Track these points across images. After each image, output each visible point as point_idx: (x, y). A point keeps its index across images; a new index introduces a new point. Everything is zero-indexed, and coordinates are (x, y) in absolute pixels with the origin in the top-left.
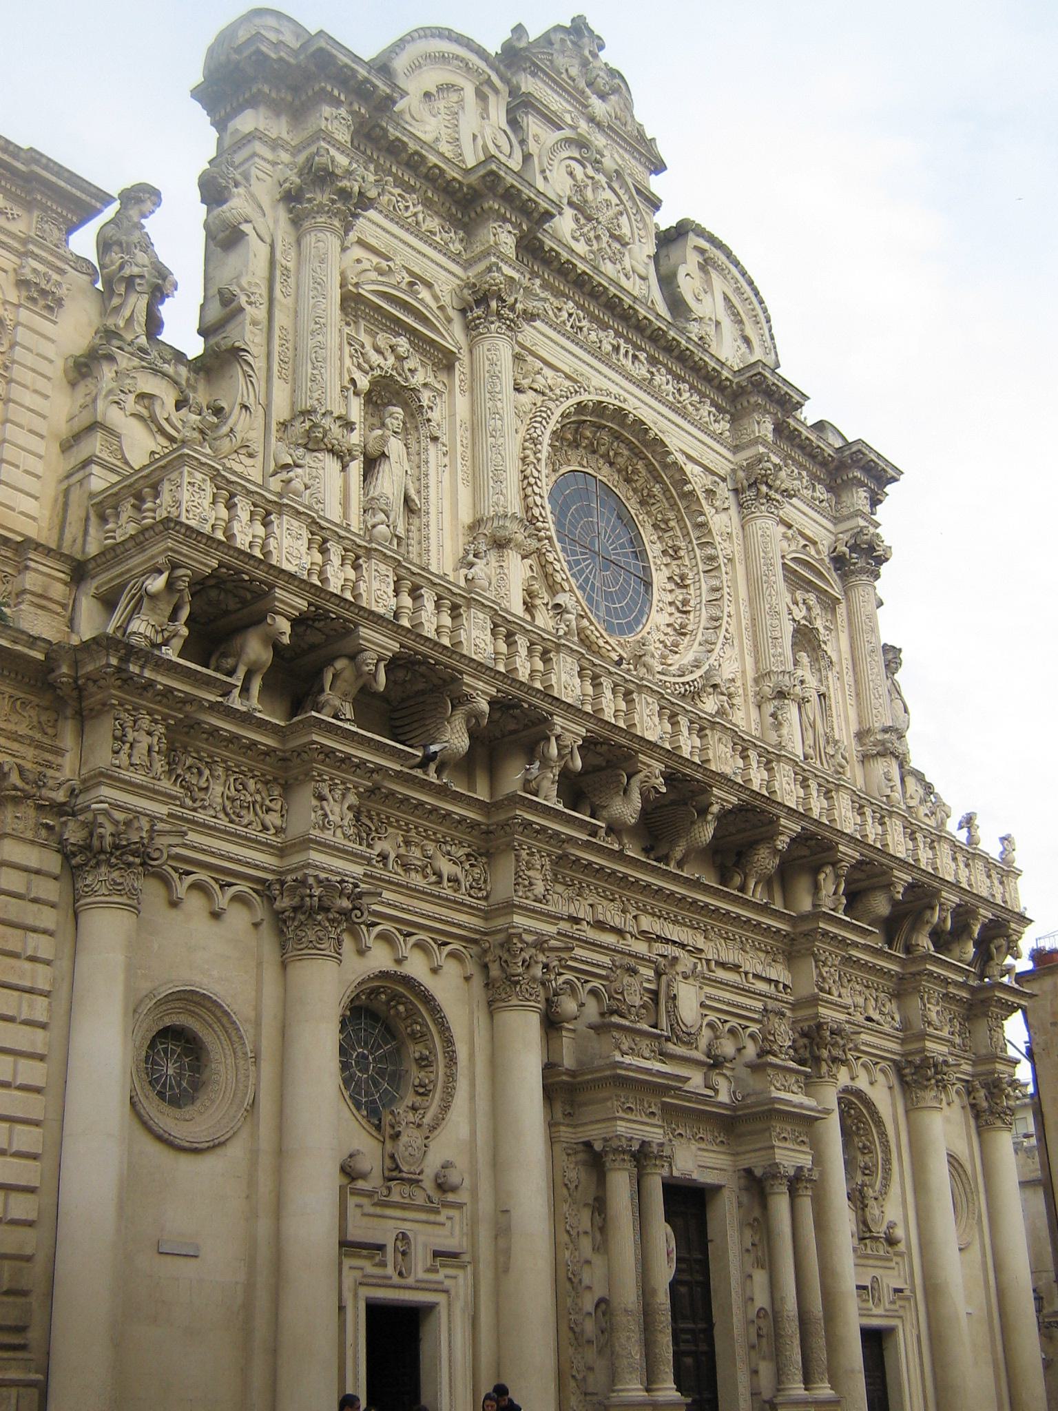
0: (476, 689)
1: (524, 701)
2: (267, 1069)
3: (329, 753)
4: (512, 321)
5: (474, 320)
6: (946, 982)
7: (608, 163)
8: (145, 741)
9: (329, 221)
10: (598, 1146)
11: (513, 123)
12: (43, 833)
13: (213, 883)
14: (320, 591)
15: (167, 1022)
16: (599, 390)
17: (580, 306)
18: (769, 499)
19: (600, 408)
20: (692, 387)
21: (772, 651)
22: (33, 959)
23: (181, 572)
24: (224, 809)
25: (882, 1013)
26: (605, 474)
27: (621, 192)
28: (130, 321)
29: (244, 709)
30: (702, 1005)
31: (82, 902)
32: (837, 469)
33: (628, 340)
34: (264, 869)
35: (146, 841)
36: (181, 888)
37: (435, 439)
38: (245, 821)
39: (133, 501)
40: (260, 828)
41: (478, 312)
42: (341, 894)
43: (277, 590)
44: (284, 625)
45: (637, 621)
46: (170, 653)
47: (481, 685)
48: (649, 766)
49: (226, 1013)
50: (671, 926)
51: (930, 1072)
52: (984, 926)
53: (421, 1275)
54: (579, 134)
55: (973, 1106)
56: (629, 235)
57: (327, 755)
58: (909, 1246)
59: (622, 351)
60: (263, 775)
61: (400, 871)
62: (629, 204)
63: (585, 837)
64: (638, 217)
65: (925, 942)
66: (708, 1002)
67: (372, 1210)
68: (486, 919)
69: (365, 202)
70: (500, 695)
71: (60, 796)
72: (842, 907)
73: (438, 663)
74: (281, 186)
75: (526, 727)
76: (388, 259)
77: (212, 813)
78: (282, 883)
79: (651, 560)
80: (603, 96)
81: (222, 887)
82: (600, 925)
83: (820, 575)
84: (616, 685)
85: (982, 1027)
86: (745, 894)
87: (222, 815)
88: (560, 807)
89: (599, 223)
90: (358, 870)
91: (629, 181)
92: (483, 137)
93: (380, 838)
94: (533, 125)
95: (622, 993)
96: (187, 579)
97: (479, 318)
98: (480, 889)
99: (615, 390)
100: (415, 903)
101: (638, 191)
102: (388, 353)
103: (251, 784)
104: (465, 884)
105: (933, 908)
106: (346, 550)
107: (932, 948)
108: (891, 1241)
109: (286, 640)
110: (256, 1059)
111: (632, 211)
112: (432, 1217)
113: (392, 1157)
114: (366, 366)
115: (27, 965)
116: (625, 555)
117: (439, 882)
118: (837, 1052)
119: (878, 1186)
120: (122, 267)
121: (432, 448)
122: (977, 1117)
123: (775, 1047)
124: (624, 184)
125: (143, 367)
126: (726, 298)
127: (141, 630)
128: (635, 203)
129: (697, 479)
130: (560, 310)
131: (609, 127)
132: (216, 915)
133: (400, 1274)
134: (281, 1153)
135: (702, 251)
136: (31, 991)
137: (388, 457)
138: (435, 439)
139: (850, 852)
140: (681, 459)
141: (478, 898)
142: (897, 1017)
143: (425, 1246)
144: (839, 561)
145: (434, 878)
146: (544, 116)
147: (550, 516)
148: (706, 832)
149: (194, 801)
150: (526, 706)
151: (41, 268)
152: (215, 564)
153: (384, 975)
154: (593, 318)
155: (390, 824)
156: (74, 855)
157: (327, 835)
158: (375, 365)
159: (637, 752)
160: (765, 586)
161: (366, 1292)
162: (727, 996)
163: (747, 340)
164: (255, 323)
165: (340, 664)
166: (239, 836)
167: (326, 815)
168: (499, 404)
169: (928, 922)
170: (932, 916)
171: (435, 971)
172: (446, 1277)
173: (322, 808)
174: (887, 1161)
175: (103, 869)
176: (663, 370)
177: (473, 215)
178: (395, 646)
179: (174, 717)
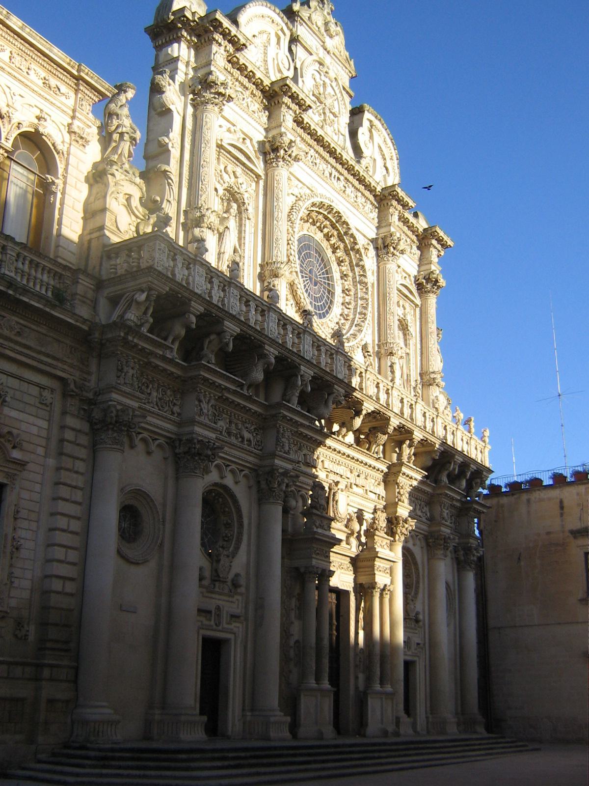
0: (270, 352)
1: (289, 358)
2: (168, 526)
3: (206, 380)
4: (289, 162)
5: (270, 159)
6: (452, 499)
7: (332, 75)
8: (131, 372)
9: (213, 108)
10: (302, 570)
11: (290, 50)
12: (82, 412)
13: (149, 438)
14: (210, 303)
15: (126, 503)
16: (321, 196)
18: (393, 254)
19: (321, 205)
21: (388, 332)
22: (77, 472)
23: (153, 292)
24: (157, 404)
25: (422, 512)
26: (319, 236)
27: (336, 89)
28: (120, 155)
29: (170, 357)
30: (348, 505)
31: (97, 447)
34: (168, 432)
35: (130, 420)
36: (137, 441)
37: (249, 219)
38: (165, 410)
39: (127, 252)
40: (171, 413)
41: (272, 155)
42: (208, 448)
43: (192, 302)
44: (194, 319)
46: (144, 330)
48: (338, 391)
49: (152, 500)
50: (337, 466)
52: (472, 473)
53: (226, 626)
54: (320, 58)
55: (457, 558)
56: (338, 112)
57: (205, 381)
58: (424, 625)
59: (333, 176)
61: (227, 436)
62: (339, 95)
64: (343, 102)
65: (445, 479)
66: (350, 504)
67: (207, 595)
69: (230, 99)
70: (280, 355)
71: (90, 395)
72: (412, 461)
73: (255, 338)
74: (190, 87)
76: (234, 125)
77: (152, 405)
78: (180, 440)
79: (335, 280)
80: (331, 37)
81: (153, 440)
84: (327, 350)
86: (370, 452)
87: (156, 407)
88: (299, 409)
89: (326, 106)
90: (213, 435)
92: (277, 60)
93: (219, 419)
94: (299, 51)
95: (317, 499)
96: (155, 296)
97: (273, 159)
98: (259, 445)
102: (232, 175)
103: (169, 392)
104: (253, 443)
105: (450, 463)
106: (220, 282)
107: (447, 482)
109: (194, 326)
110: (164, 521)
112: (231, 599)
113: (216, 571)
114: (222, 182)
115: (75, 476)
116: (324, 278)
117: (242, 442)
119: (413, 594)
120: (118, 127)
121: (247, 221)
124: (338, 84)
125: (127, 180)
126: (380, 147)
127: (132, 319)
128: (342, 95)
129: (362, 242)
131: (334, 54)
132: (149, 453)
133: (216, 624)
135: (371, 121)
136: (75, 487)
137: (229, 229)
138: (249, 219)
141: (257, 450)
142: (428, 515)
144: (420, 287)
145: (240, 440)
146: (304, 47)
147: (297, 260)
150: (290, 360)
151: (81, 125)
152: (168, 289)
153: (216, 484)
155: (223, 412)
156: (96, 424)
157: (202, 419)
158: (226, 181)
159: (334, 384)
160: (388, 298)
161: (202, 632)
163: (387, 169)
164: (174, 158)
165: (213, 337)
166: (163, 417)
167: (201, 409)
168: (280, 204)
169: (447, 470)
170: (450, 467)
171: (236, 483)
172: (235, 627)
173: (200, 406)
175: (110, 432)
176: (350, 186)
177: (273, 104)
178: (238, 330)
179: (143, 361)
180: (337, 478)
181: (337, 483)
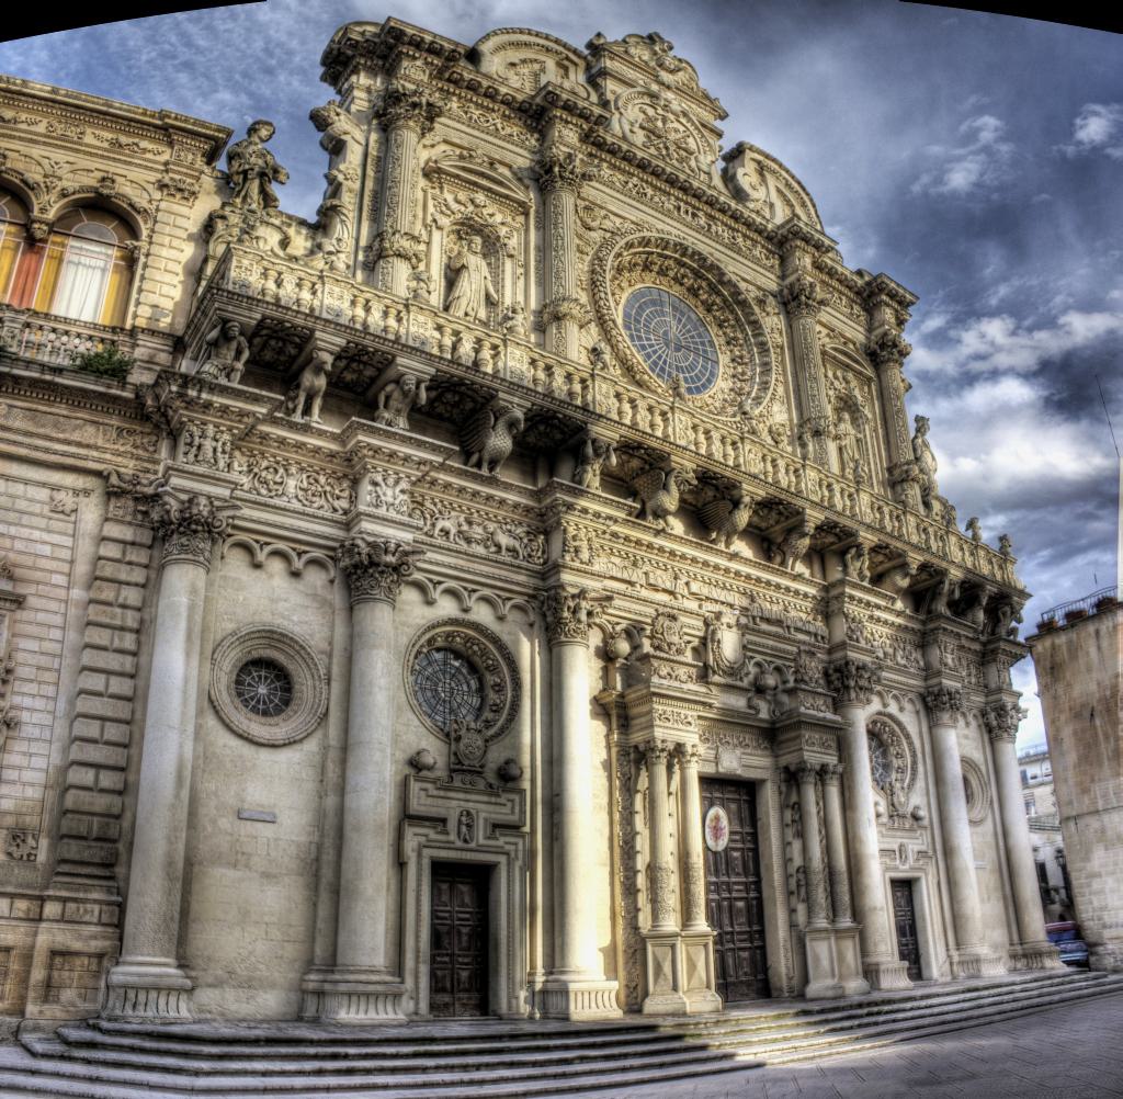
0: (511, 403)
2: (336, 687)
7: (675, 106)
10: (642, 747)
13: (290, 551)
17: (642, 180)
18: (807, 305)
20: (745, 236)
24: (297, 497)
27: (689, 125)
30: (744, 647)
32: (869, 296)
33: (686, 203)
38: (316, 505)
42: (386, 552)
45: (705, 387)
47: (516, 400)
51: (946, 698)
52: (990, 597)
60: (334, 473)
63: (624, 516)
68: (543, 579)
75: (571, 437)
82: (655, 588)
83: (856, 361)
85: (992, 670)
87: (294, 501)
91: (694, 118)
99: (675, 232)
100: (476, 566)
101: (703, 125)
103: (322, 479)
108: (916, 818)
111: (695, 132)
118: (863, 683)
122: (990, 731)
123: (806, 678)
124: (690, 120)
126: (779, 190)
129: (751, 294)
130: (627, 183)
132: (296, 574)
134: (345, 748)
139: (869, 536)
140: (734, 278)
142: (922, 663)
143: (486, 820)
145: (493, 549)
146: (615, 77)
148: (743, 517)
149: (270, 491)
154: (655, 188)
155: (453, 509)
162: (771, 643)
165: (389, 388)
167: (378, 496)
171: (501, 619)
174: (914, 763)
180: (717, 608)
181: (718, 615)
